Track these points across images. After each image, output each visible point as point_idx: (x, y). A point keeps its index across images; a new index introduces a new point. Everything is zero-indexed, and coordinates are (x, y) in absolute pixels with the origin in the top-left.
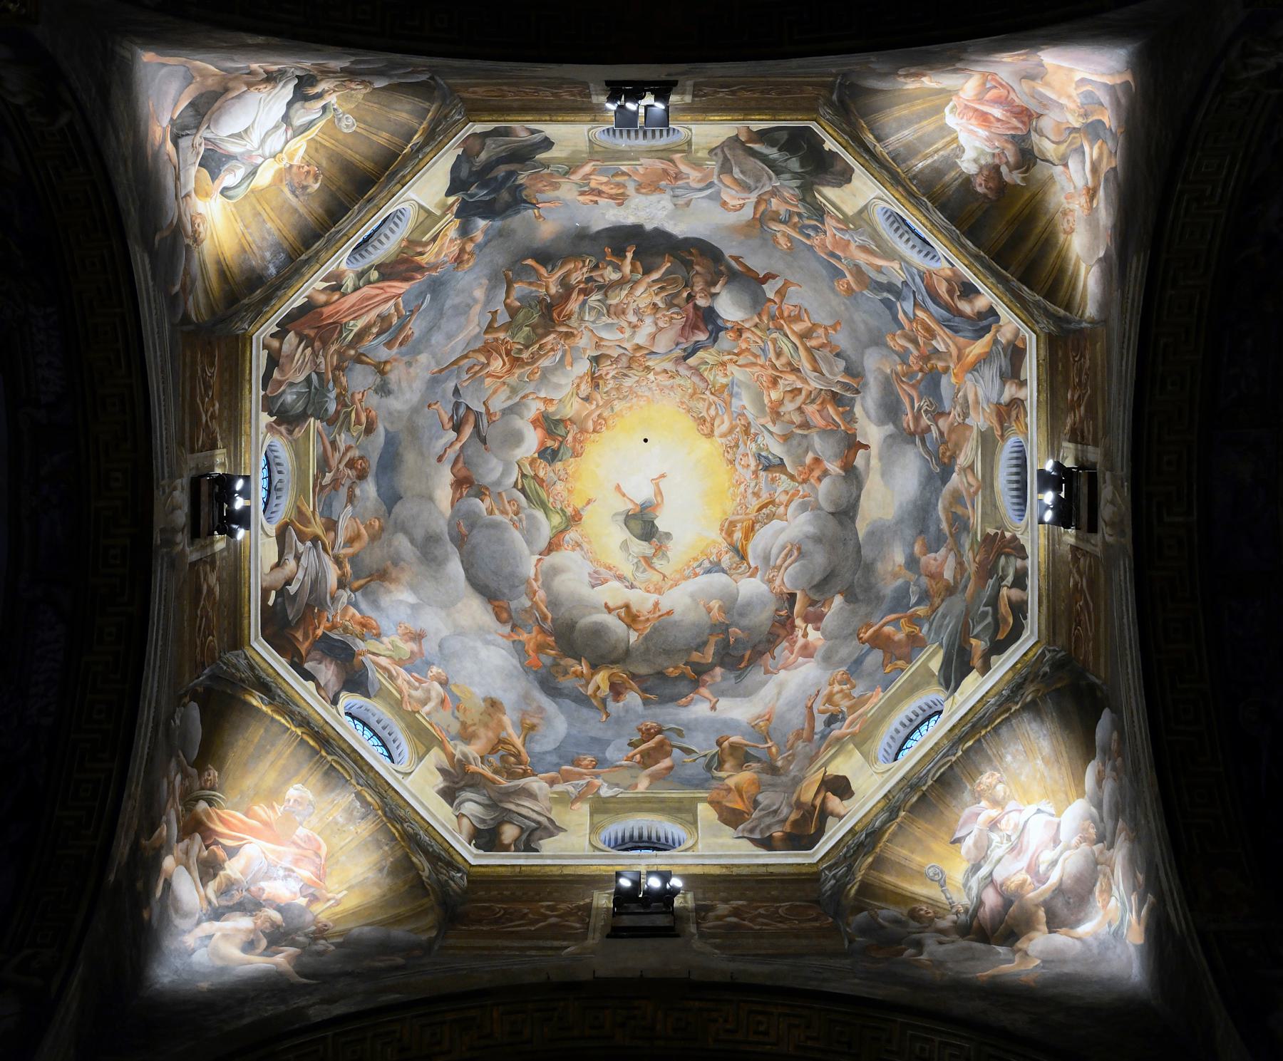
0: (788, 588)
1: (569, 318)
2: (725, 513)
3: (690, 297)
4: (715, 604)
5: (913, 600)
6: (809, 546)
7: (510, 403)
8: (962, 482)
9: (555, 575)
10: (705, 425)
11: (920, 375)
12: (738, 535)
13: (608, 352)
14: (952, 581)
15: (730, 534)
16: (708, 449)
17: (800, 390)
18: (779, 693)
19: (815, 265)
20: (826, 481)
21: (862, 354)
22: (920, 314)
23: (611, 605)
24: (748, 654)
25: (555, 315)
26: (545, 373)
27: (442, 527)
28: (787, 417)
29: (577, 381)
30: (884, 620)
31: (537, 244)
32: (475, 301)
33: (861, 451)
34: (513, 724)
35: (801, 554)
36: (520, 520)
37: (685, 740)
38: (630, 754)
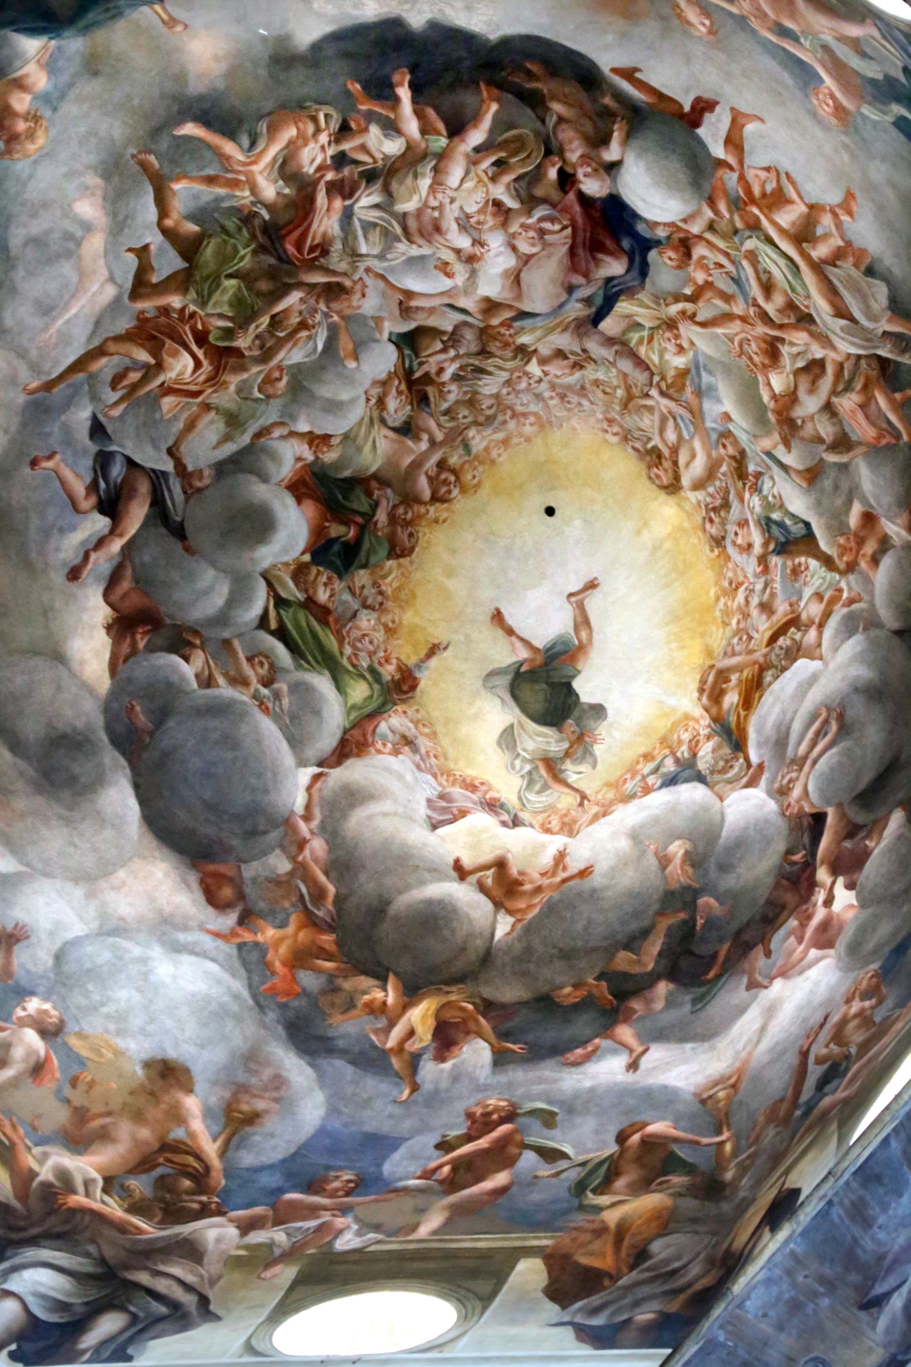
1: (325, 252)
2: (709, 653)
3: (566, 179)
4: (677, 849)
6: (858, 710)
7: (230, 448)
9: (352, 806)
12: (731, 699)
13: (432, 322)
15: (716, 696)
16: (669, 518)
18: (763, 1029)
20: (887, 562)
23: (468, 862)
25: (290, 249)
27: (87, 713)
28: (809, 427)
29: (376, 391)
31: (196, 87)
32: (87, 227)
34: (208, 1113)
35: (845, 729)
36: (277, 696)
37: (557, 1133)
38: (433, 1165)
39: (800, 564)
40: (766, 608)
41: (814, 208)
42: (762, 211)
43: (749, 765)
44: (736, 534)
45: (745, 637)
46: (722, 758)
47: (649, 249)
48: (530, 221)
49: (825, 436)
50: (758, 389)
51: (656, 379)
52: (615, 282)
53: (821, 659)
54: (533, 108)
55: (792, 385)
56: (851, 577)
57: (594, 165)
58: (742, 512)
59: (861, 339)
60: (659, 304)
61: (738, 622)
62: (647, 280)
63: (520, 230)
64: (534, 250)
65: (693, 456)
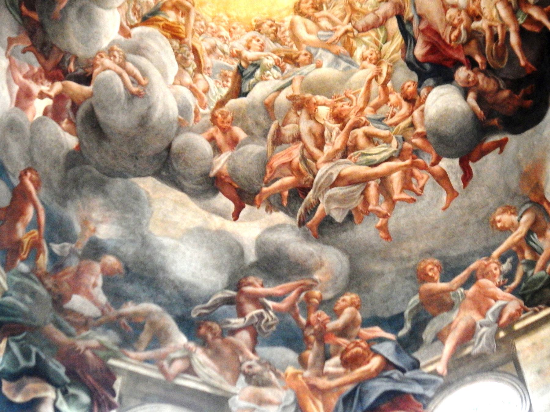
0: (99, 75)
3: (472, 64)
5: (56, 248)
8: (176, 349)
11: (303, 321)
12: (172, 17)
14: (68, 305)
15: (176, 8)
17: (320, 147)
19: (465, 246)
20: (208, 148)
21: (344, 251)
22: (375, 362)
24: (35, 16)
30: (40, 207)
33: (231, 206)
35: (132, 96)
39: (227, 81)
40: (211, 51)
41: (392, 203)
42: (406, 166)
43: (132, 27)
44: (258, 41)
45: (202, 30)
46: (142, 8)
47: (419, 78)
48: (462, 27)
49: (285, 127)
50: (325, 96)
51: (356, 33)
52: (412, 44)
53: (174, 84)
54: (512, 80)
55: (318, 120)
56: (209, 117)
57: (471, 85)
58: (269, 49)
59: (322, 184)
60: (391, 61)
61: (212, 28)
62: (405, 64)
63: (460, 17)
64: (448, 16)
65: (309, 32)
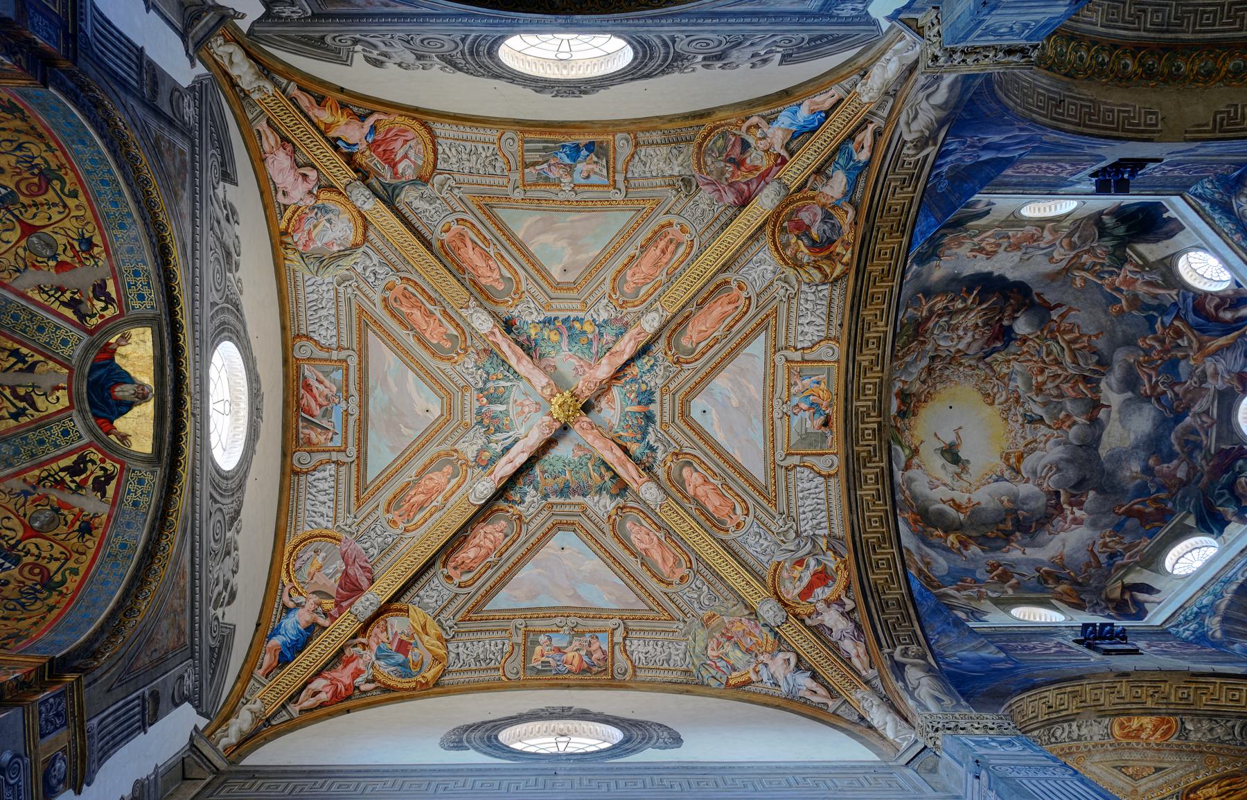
3: (1001, 320)
10: (989, 398)
16: (991, 413)
20: (1075, 428)
26: (908, 364)
31: (927, 284)
